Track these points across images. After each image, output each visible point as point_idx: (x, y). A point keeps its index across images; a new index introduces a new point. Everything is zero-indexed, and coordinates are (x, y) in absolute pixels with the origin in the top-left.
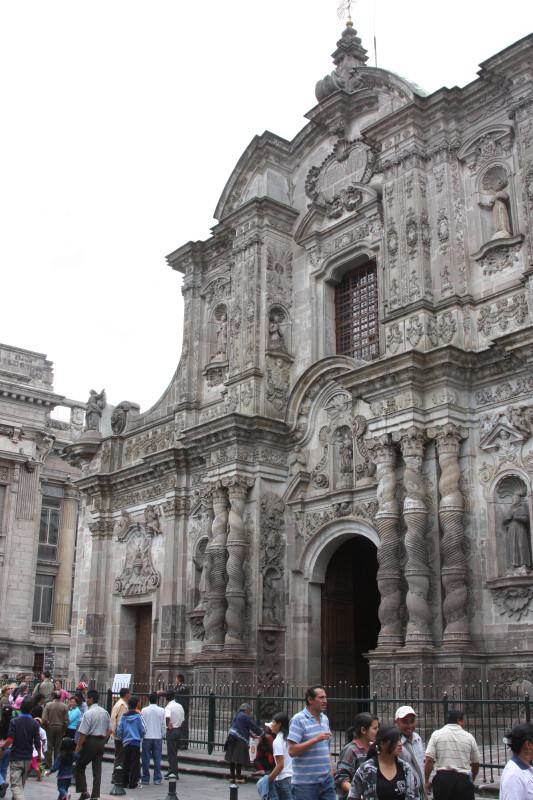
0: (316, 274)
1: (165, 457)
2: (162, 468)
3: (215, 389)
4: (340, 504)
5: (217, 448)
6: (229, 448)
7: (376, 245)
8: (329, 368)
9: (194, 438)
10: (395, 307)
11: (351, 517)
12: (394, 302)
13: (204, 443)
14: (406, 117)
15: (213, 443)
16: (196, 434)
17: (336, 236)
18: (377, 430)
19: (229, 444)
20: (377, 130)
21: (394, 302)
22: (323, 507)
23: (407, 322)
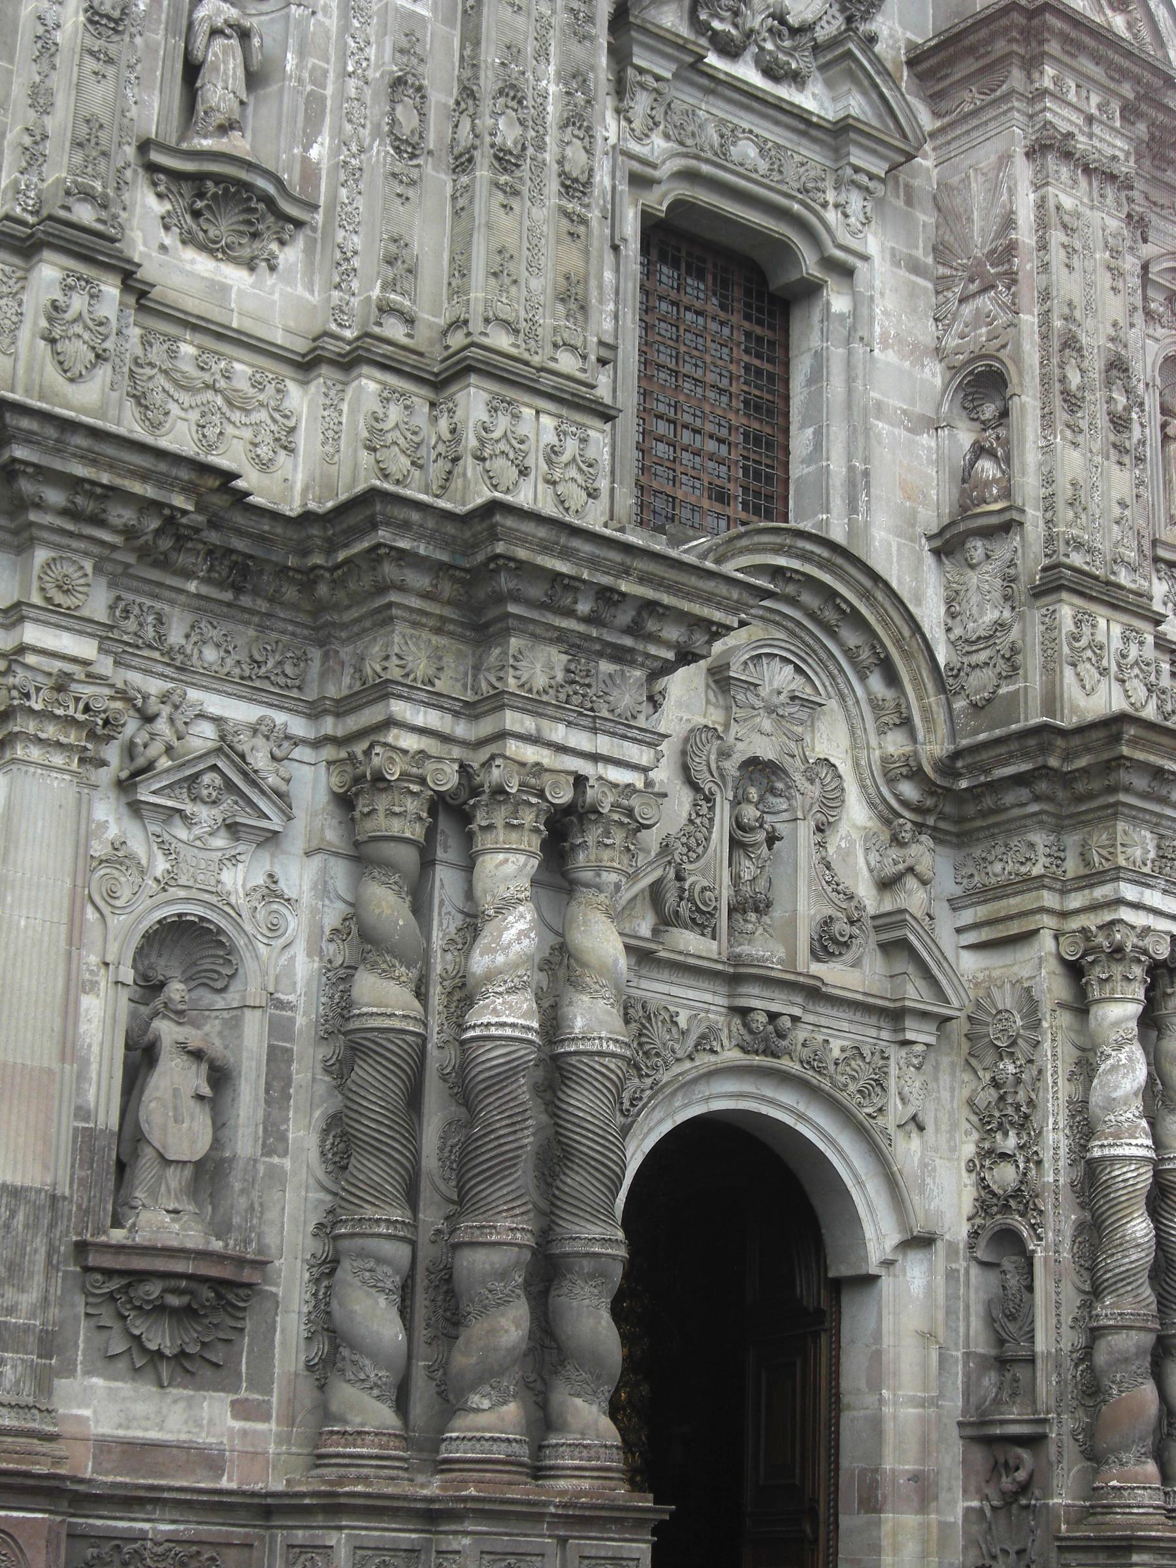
0: (636, 166)
1: (144, 476)
2: (55, 497)
3: (202, 264)
4: (773, 1016)
5: (561, 638)
6: (606, 667)
7: (850, 259)
8: (795, 564)
9: (522, 554)
10: (1077, 559)
11: (785, 1063)
12: (1079, 546)
13: (536, 591)
14: (1138, 80)
15: (570, 613)
16: (545, 548)
17: (721, 110)
18: (1137, 906)
19: (621, 655)
20: (1073, 34)
21: (1079, 546)
22: (691, 994)
23: (1116, 630)
